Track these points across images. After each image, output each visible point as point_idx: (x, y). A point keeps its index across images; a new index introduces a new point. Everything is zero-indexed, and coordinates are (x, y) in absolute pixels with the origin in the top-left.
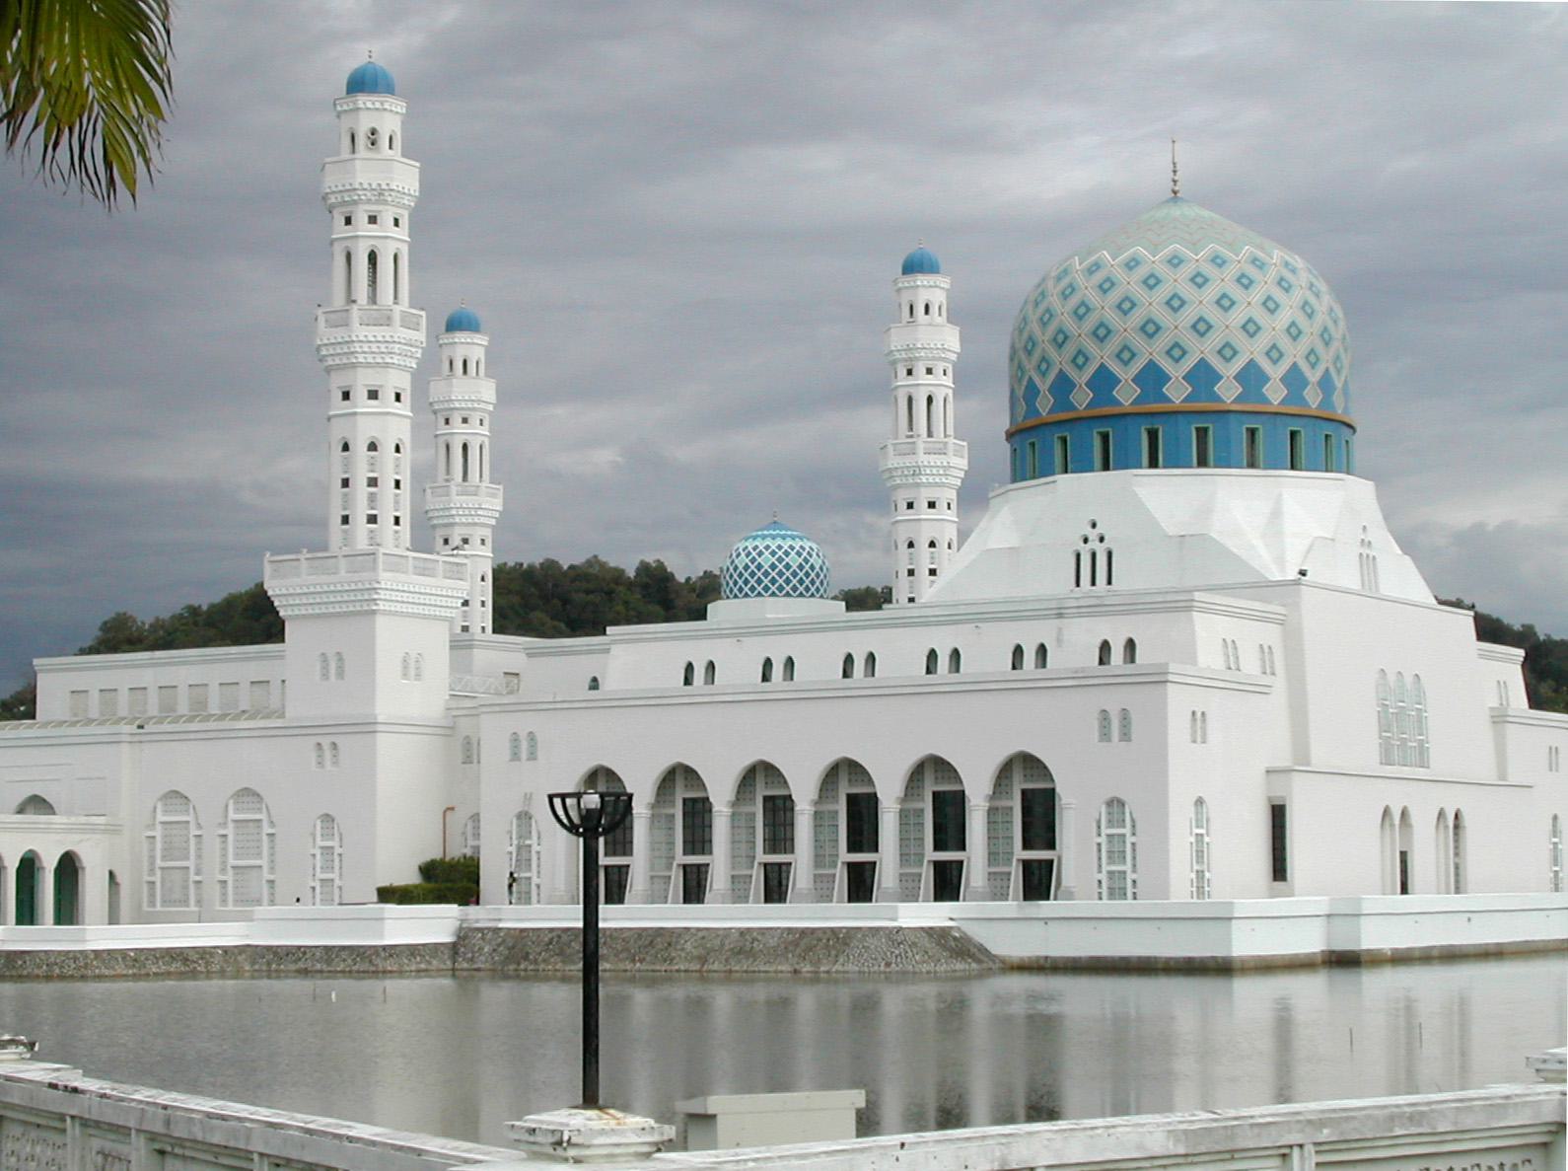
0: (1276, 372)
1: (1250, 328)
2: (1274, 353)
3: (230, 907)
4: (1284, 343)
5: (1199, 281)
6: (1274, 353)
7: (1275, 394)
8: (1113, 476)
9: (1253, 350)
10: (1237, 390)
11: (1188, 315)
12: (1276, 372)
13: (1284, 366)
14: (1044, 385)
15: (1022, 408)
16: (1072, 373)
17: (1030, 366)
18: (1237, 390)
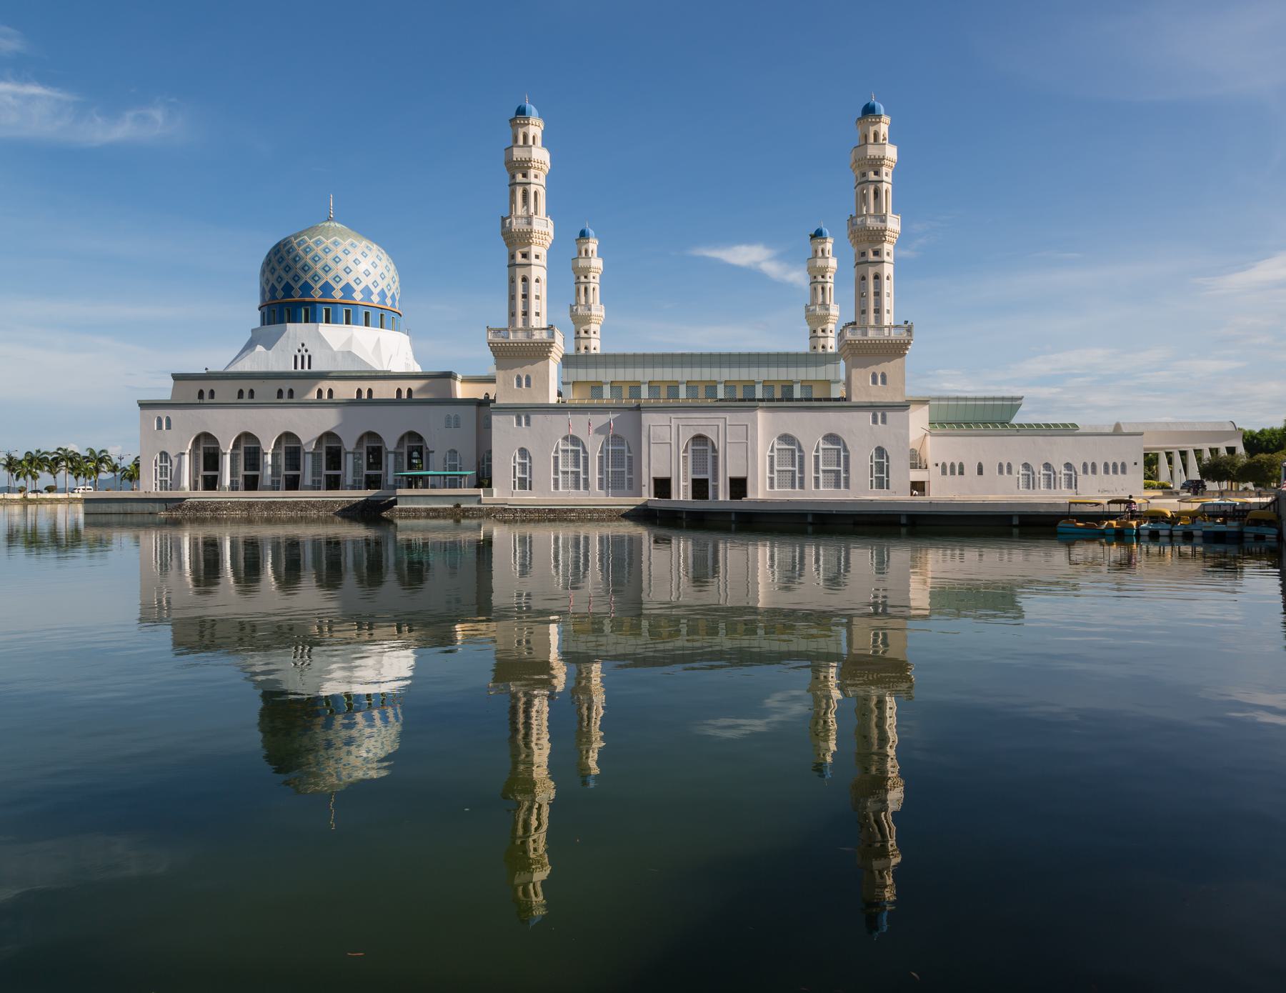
0: (376, 291)
1: (367, 274)
2: (375, 283)
3: (223, 494)
4: (379, 280)
5: (346, 252)
6: (375, 283)
7: (375, 299)
8: (311, 325)
9: (367, 281)
10: (361, 296)
11: (341, 266)
12: (376, 291)
13: (379, 289)
14: (280, 287)
15: (268, 296)
16: (292, 283)
17: (273, 280)
18: (361, 296)
